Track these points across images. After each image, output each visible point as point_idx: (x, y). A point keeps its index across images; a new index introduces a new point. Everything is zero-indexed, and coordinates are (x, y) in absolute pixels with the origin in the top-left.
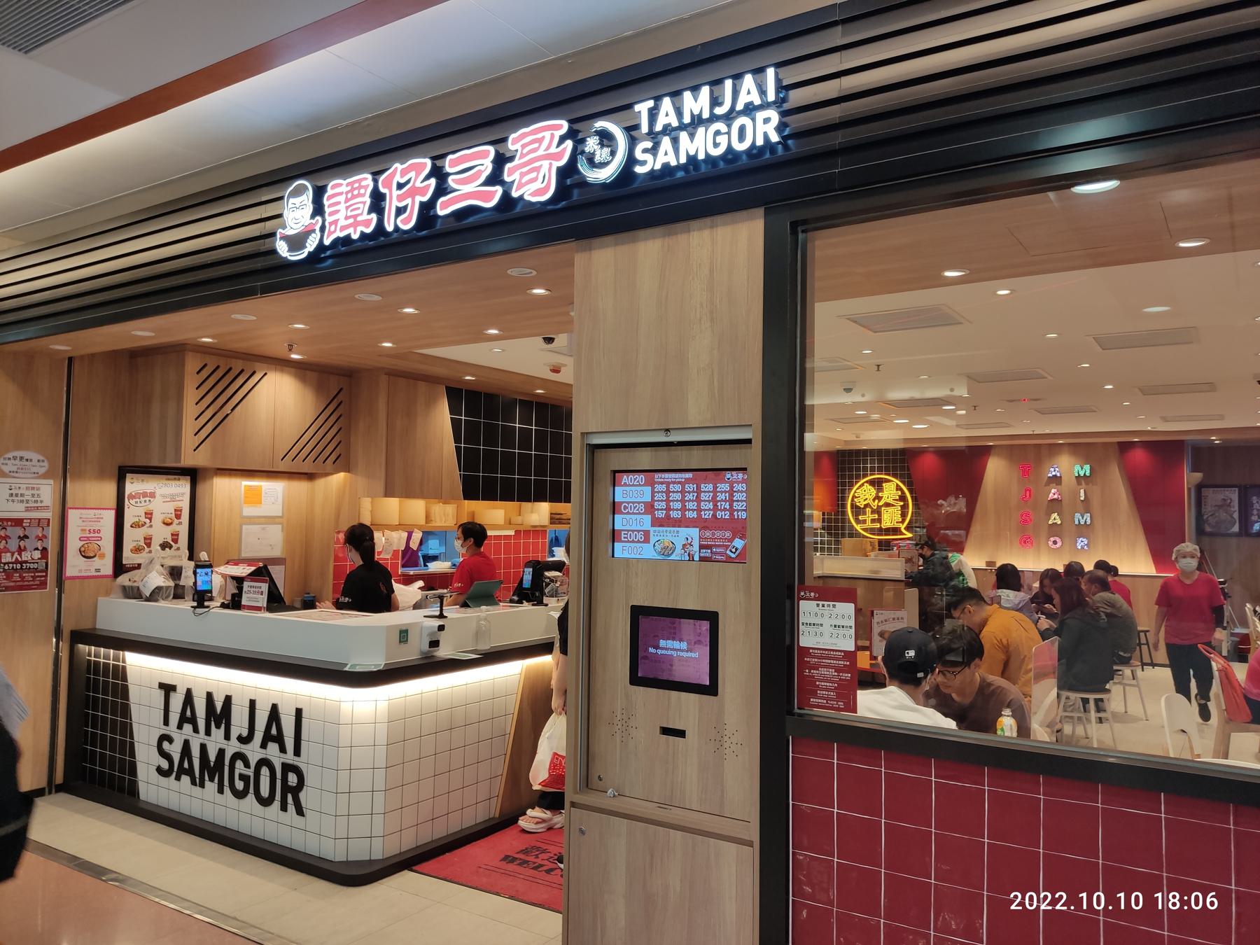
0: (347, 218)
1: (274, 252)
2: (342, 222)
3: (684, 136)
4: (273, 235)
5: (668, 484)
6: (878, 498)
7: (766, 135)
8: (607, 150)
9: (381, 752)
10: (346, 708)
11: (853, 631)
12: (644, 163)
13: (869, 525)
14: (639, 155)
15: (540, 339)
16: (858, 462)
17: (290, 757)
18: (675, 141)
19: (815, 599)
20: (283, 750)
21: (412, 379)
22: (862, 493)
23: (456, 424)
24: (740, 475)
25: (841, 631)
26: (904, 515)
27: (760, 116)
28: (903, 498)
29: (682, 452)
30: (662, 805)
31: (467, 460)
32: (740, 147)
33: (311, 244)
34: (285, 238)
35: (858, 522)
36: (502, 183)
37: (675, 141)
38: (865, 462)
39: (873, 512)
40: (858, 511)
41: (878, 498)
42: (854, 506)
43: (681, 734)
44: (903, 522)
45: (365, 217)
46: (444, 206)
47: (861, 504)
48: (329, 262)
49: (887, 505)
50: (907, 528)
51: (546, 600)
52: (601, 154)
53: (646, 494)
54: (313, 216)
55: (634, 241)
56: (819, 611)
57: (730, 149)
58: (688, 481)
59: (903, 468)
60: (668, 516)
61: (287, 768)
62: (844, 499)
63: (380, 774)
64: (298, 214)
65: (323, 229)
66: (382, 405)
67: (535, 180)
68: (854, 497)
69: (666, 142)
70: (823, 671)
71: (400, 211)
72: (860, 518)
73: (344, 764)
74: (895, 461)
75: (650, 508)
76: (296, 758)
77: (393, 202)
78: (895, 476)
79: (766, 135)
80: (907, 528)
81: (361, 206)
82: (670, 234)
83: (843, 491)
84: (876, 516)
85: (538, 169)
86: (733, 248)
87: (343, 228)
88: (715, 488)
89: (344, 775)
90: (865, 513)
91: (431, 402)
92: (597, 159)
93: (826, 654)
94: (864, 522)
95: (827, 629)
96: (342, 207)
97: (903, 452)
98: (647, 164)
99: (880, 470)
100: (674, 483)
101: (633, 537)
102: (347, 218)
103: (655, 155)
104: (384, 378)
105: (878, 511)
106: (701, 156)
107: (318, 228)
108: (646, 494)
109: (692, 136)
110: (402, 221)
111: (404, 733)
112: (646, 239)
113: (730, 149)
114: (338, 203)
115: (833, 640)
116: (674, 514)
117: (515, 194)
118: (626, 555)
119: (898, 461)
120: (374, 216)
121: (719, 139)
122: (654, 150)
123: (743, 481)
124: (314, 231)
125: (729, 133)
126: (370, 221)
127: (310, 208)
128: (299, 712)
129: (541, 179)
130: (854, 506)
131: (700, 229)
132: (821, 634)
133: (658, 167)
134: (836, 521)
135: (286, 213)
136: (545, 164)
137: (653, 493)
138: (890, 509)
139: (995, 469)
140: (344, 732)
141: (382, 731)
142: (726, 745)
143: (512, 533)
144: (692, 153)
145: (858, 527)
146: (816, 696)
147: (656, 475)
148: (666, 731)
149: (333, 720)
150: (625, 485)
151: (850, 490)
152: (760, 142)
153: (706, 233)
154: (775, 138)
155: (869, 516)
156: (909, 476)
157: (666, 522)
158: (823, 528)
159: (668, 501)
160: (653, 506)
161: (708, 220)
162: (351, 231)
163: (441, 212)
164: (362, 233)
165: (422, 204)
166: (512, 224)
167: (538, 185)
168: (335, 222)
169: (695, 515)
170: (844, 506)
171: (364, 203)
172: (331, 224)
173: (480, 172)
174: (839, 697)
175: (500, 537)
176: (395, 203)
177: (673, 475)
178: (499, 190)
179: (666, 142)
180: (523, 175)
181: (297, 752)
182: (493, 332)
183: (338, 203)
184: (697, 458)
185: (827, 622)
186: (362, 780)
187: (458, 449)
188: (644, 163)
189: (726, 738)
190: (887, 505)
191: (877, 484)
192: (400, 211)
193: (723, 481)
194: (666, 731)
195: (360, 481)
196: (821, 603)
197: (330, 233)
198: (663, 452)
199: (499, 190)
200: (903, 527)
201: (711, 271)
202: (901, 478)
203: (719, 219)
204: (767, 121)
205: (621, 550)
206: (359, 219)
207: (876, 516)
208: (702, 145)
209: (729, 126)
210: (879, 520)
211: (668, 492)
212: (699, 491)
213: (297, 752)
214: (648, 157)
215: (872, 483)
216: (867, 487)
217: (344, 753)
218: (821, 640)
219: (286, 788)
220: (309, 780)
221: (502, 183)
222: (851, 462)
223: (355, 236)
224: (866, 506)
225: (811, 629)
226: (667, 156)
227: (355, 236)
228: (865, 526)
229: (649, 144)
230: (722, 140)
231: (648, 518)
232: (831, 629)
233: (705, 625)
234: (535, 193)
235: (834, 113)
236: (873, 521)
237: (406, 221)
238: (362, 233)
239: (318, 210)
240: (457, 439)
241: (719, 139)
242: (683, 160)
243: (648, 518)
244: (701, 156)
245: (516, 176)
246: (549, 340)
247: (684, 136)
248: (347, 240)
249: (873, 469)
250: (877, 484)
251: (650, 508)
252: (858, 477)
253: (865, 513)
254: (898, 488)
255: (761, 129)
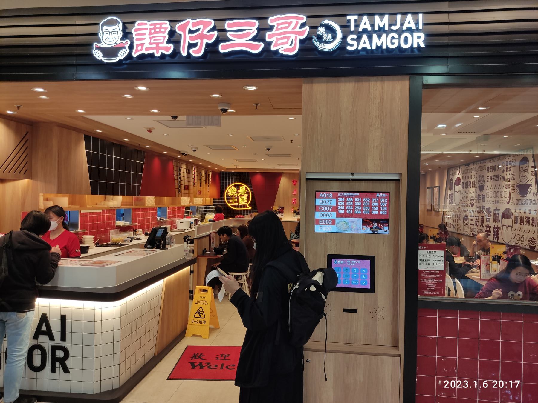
0: (150, 43)
1: (92, 55)
2: (147, 45)
3: (375, 36)
4: (91, 45)
5: (346, 198)
6: (237, 192)
7: (418, 43)
8: (330, 35)
9: (117, 333)
10: (98, 312)
11: (443, 262)
12: (352, 45)
13: (234, 204)
14: (349, 40)
15: (170, 118)
16: (229, 177)
17: (57, 342)
18: (370, 38)
19: (426, 249)
20: (52, 338)
21: (69, 129)
22: (231, 190)
23: (88, 154)
24: (384, 195)
25: (438, 263)
26: (248, 200)
27: (416, 34)
28: (248, 193)
29: (357, 184)
30: (346, 344)
31: (93, 173)
32: (404, 46)
33: (122, 55)
34: (102, 50)
35: (229, 202)
36: (263, 40)
37: (370, 38)
38: (232, 177)
39: (235, 198)
40: (229, 198)
41: (237, 192)
42: (227, 196)
43: (355, 311)
44: (247, 203)
45: (165, 45)
46: (224, 47)
47: (230, 195)
48: (125, 66)
49: (241, 195)
50: (250, 205)
51: (167, 246)
52: (327, 37)
53: (333, 202)
54: (123, 38)
55: (338, 82)
56: (428, 254)
57: (399, 47)
58: (356, 197)
59: (248, 181)
60: (345, 213)
61: (54, 349)
62: (223, 193)
63: (117, 345)
64: (111, 36)
65: (131, 47)
66: (55, 142)
67: (286, 43)
68: (227, 192)
69: (365, 37)
70: (430, 280)
71: (191, 46)
72: (230, 201)
73: (97, 342)
74: (245, 177)
75: (335, 209)
76: (62, 342)
77: (186, 39)
78: (245, 183)
79: (418, 43)
80: (250, 205)
81: (162, 38)
82: (358, 81)
83: (223, 190)
84: (237, 200)
85: (288, 38)
86: (395, 91)
87: (147, 49)
88: (371, 200)
89: (98, 348)
90: (232, 199)
91: (77, 143)
92: (325, 38)
93: (431, 272)
94: (232, 202)
95: (431, 262)
96: (147, 37)
97: (248, 173)
98: (353, 45)
99: (238, 181)
100: (349, 197)
101: (326, 222)
102: (150, 43)
103: (359, 43)
104: (56, 129)
105: (237, 198)
106: (384, 47)
107: (127, 46)
108: (333, 202)
109: (379, 37)
110: (193, 51)
111: (128, 320)
112: (345, 82)
113: (399, 47)
114: (145, 34)
115: (434, 267)
116: (349, 212)
117: (273, 48)
118: (322, 230)
119: (246, 177)
120: (172, 46)
121: (394, 41)
122: (358, 39)
123: (386, 197)
124: (124, 48)
125: (399, 39)
126: (169, 48)
127: (121, 34)
128: (63, 318)
129: (289, 43)
130: (227, 196)
131: (375, 81)
132: (429, 264)
133: (360, 48)
134: (220, 202)
135: (100, 35)
136: (293, 37)
137: (337, 202)
138: (242, 197)
139: (284, 182)
140: (97, 325)
141: (118, 322)
142: (378, 314)
143: (101, 211)
144: (379, 45)
145: (229, 205)
146: (426, 290)
147: (339, 194)
148: (346, 310)
149: (89, 321)
150: (321, 198)
151: (226, 189)
152: (415, 46)
153: (379, 84)
154: (423, 46)
155: (233, 200)
156: (251, 184)
157: (346, 215)
158: (214, 205)
159: (345, 205)
160: (337, 208)
161: (380, 78)
162: (154, 51)
163: (222, 51)
164: (162, 54)
165: (208, 45)
166: (266, 65)
167: (287, 46)
168: (142, 45)
169: (360, 212)
170: (223, 196)
171: (165, 37)
172: (138, 45)
173: (249, 34)
174: (437, 290)
175: (90, 213)
176: (188, 40)
177: (349, 194)
178: (262, 45)
179: (365, 37)
180: (278, 39)
181: (63, 338)
182: (155, 111)
183: (145, 34)
184: (364, 186)
185: (431, 259)
186: (107, 349)
187: (89, 168)
188: (352, 45)
189: (378, 311)
190: (241, 195)
191: (237, 187)
192: (191, 46)
193: (375, 197)
194: (346, 310)
195: (40, 185)
196: (429, 251)
197: (137, 51)
198: (345, 184)
199: (262, 45)
200: (248, 205)
201: (381, 101)
202: (247, 184)
203: (385, 78)
204: (419, 37)
205: (318, 228)
206: (160, 45)
207: (237, 200)
208: (384, 42)
209: (400, 36)
210: (238, 202)
211: (345, 202)
212: (362, 202)
213: (63, 338)
214: (355, 43)
215: (235, 186)
216: (233, 188)
217: (97, 337)
218: (429, 266)
219: (54, 359)
220: (72, 353)
221: (263, 40)
222: (226, 177)
223: (157, 55)
224: (233, 196)
225: (424, 262)
226: (364, 43)
227: (157, 55)
228: (232, 204)
229: (355, 37)
230: (396, 42)
231: (334, 214)
232: (434, 262)
233: (368, 262)
234: (285, 50)
235: (445, 40)
236: (235, 202)
237: (198, 51)
238: (162, 54)
239: (126, 34)
240: (89, 164)
241: (394, 41)
242: (374, 47)
243: (334, 214)
244: (384, 47)
245: (274, 39)
246: (175, 117)
247: (375, 36)
248: (152, 55)
249: (235, 181)
250: (237, 187)
251: (335, 209)
252: (229, 184)
253: (232, 199)
254: (246, 189)
255: (416, 40)
